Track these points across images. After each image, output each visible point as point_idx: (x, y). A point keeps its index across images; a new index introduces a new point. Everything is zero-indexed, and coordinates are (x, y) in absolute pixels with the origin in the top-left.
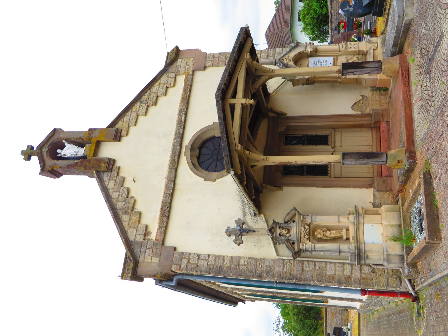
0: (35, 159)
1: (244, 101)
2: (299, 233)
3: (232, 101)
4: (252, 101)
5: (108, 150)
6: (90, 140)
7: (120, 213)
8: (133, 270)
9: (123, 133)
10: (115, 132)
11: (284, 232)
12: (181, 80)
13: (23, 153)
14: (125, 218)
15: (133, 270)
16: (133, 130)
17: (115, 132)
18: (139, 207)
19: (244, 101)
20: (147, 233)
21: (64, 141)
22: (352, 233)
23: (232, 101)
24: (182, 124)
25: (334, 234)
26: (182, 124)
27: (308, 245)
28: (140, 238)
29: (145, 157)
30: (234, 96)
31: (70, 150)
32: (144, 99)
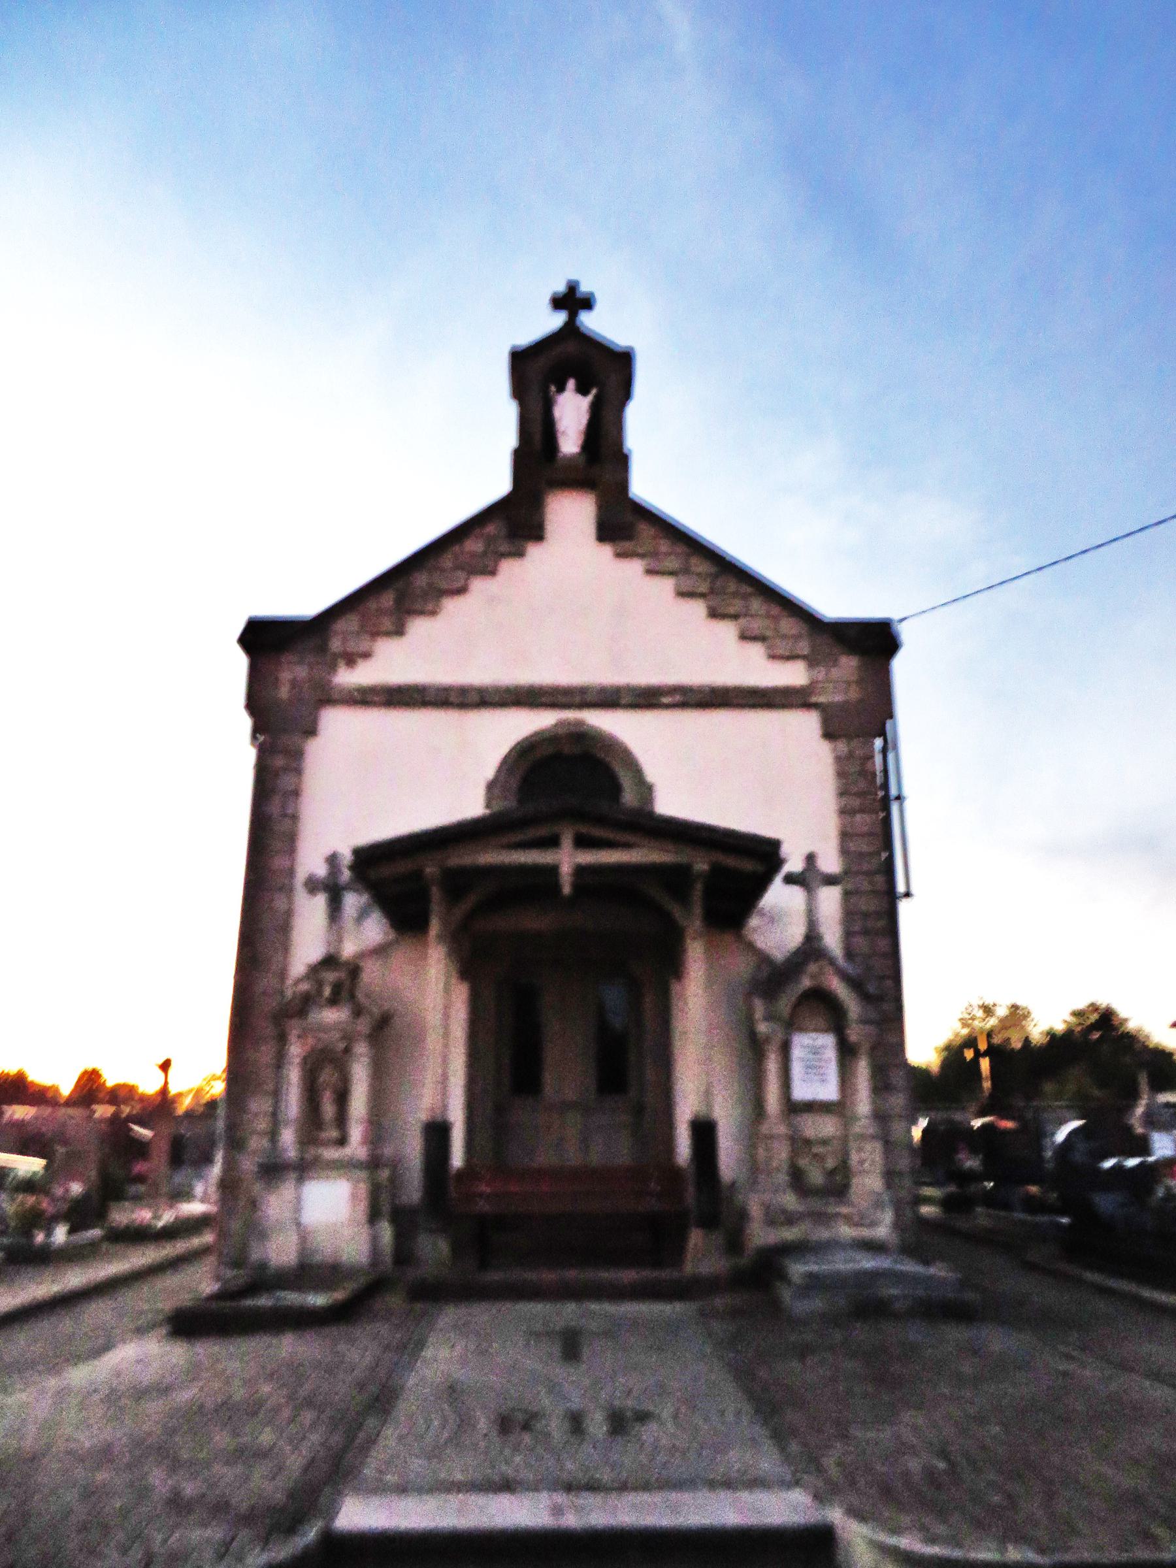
0: (558, 319)
1: (566, 869)
2: (324, 1028)
3: (567, 842)
4: (567, 890)
5: (571, 514)
6: (604, 459)
7: (400, 584)
8: (264, 639)
9: (627, 545)
10: (627, 524)
11: (327, 991)
12: (794, 675)
13: (572, 288)
14: (387, 599)
15: (264, 639)
16: (635, 567)
17: (627, 524)
18: (419, 628)
19: (566, 869)
20: (351, 660)
21: (594, 391)
22: (331, 1154)
23: (567, 842)
24: (647, 699)
25: (328, 1109)
26: (647, 699)
27: (296, 1050)
28: (335, 645)
29: (570, 614)
30: (582, 842)
31: (571, 412)
32: (724, 583)
